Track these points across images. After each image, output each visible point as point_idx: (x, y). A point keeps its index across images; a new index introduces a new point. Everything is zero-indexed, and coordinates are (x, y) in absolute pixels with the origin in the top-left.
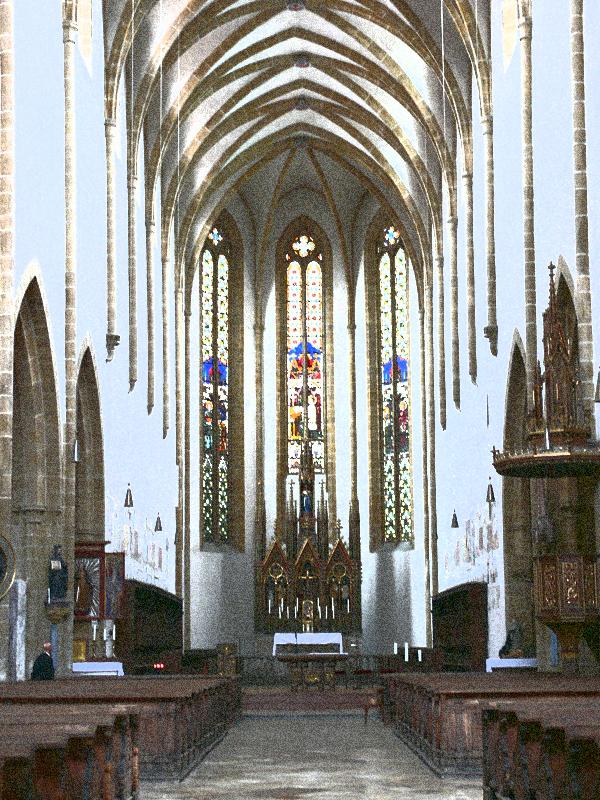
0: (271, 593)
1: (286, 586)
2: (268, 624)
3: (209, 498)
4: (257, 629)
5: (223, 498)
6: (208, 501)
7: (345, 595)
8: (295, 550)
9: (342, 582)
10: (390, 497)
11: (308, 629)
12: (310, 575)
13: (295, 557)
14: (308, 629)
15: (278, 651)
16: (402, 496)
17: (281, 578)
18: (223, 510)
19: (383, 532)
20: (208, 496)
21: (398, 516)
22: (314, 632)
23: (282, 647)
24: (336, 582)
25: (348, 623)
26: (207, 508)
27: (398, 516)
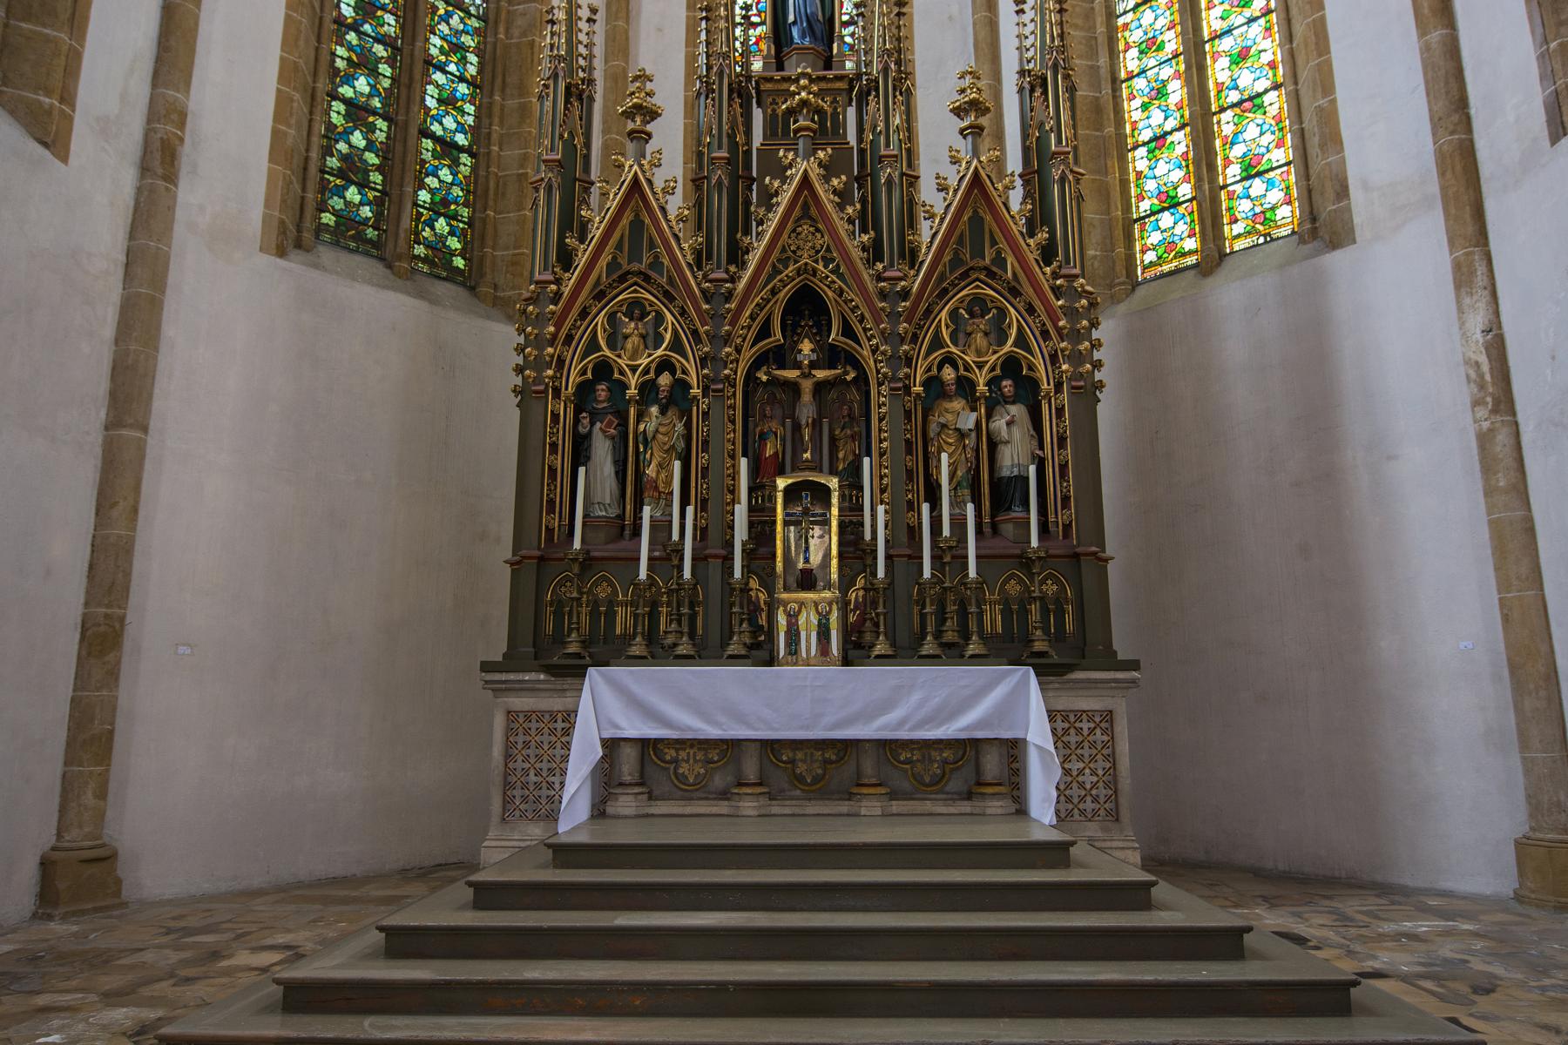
0: (602, 450)
1: (685, 414)
2: (565, 612)
3: (374, 73)
4: (511, 661)
5: (448, 101)
6: (362, 84)
7: (1015, 456)
8: (740, 220)
9: (993, 383)
10: (1159, 92)
11: (809, 641)
12: (831, 356)
13: (737, 255)
14: (809, 641)
15: (606, 780)
16: (1219, 71)
17: (665, 365)
18: (447, 148)
19: (1129, 239)
20: (364, 63)
21: (1203, 161)
22: (846, 662)
23: (642, 765)
24: (965, 387)
25: (1055, 622)
26: (357, 112)
27: (1203, 161)
